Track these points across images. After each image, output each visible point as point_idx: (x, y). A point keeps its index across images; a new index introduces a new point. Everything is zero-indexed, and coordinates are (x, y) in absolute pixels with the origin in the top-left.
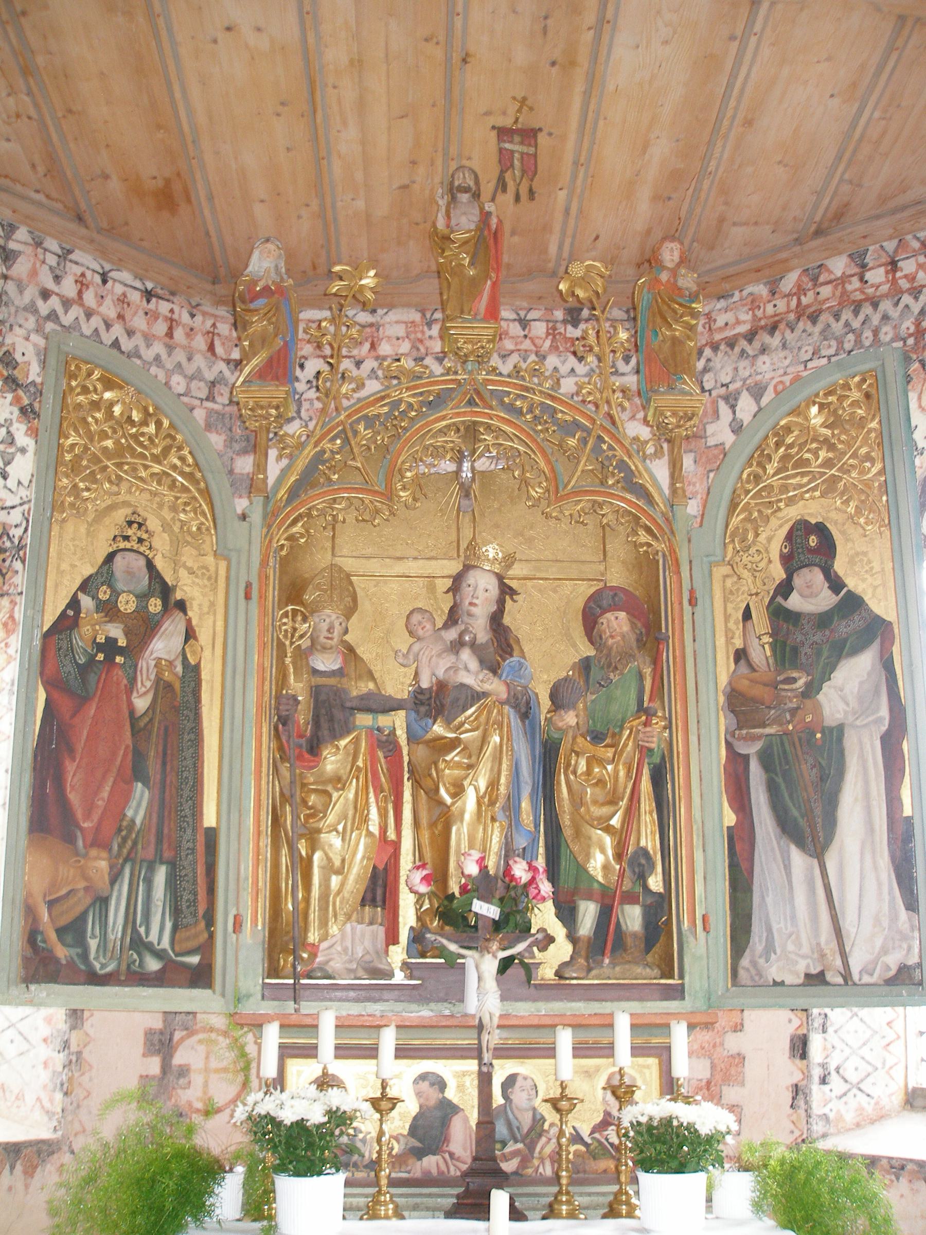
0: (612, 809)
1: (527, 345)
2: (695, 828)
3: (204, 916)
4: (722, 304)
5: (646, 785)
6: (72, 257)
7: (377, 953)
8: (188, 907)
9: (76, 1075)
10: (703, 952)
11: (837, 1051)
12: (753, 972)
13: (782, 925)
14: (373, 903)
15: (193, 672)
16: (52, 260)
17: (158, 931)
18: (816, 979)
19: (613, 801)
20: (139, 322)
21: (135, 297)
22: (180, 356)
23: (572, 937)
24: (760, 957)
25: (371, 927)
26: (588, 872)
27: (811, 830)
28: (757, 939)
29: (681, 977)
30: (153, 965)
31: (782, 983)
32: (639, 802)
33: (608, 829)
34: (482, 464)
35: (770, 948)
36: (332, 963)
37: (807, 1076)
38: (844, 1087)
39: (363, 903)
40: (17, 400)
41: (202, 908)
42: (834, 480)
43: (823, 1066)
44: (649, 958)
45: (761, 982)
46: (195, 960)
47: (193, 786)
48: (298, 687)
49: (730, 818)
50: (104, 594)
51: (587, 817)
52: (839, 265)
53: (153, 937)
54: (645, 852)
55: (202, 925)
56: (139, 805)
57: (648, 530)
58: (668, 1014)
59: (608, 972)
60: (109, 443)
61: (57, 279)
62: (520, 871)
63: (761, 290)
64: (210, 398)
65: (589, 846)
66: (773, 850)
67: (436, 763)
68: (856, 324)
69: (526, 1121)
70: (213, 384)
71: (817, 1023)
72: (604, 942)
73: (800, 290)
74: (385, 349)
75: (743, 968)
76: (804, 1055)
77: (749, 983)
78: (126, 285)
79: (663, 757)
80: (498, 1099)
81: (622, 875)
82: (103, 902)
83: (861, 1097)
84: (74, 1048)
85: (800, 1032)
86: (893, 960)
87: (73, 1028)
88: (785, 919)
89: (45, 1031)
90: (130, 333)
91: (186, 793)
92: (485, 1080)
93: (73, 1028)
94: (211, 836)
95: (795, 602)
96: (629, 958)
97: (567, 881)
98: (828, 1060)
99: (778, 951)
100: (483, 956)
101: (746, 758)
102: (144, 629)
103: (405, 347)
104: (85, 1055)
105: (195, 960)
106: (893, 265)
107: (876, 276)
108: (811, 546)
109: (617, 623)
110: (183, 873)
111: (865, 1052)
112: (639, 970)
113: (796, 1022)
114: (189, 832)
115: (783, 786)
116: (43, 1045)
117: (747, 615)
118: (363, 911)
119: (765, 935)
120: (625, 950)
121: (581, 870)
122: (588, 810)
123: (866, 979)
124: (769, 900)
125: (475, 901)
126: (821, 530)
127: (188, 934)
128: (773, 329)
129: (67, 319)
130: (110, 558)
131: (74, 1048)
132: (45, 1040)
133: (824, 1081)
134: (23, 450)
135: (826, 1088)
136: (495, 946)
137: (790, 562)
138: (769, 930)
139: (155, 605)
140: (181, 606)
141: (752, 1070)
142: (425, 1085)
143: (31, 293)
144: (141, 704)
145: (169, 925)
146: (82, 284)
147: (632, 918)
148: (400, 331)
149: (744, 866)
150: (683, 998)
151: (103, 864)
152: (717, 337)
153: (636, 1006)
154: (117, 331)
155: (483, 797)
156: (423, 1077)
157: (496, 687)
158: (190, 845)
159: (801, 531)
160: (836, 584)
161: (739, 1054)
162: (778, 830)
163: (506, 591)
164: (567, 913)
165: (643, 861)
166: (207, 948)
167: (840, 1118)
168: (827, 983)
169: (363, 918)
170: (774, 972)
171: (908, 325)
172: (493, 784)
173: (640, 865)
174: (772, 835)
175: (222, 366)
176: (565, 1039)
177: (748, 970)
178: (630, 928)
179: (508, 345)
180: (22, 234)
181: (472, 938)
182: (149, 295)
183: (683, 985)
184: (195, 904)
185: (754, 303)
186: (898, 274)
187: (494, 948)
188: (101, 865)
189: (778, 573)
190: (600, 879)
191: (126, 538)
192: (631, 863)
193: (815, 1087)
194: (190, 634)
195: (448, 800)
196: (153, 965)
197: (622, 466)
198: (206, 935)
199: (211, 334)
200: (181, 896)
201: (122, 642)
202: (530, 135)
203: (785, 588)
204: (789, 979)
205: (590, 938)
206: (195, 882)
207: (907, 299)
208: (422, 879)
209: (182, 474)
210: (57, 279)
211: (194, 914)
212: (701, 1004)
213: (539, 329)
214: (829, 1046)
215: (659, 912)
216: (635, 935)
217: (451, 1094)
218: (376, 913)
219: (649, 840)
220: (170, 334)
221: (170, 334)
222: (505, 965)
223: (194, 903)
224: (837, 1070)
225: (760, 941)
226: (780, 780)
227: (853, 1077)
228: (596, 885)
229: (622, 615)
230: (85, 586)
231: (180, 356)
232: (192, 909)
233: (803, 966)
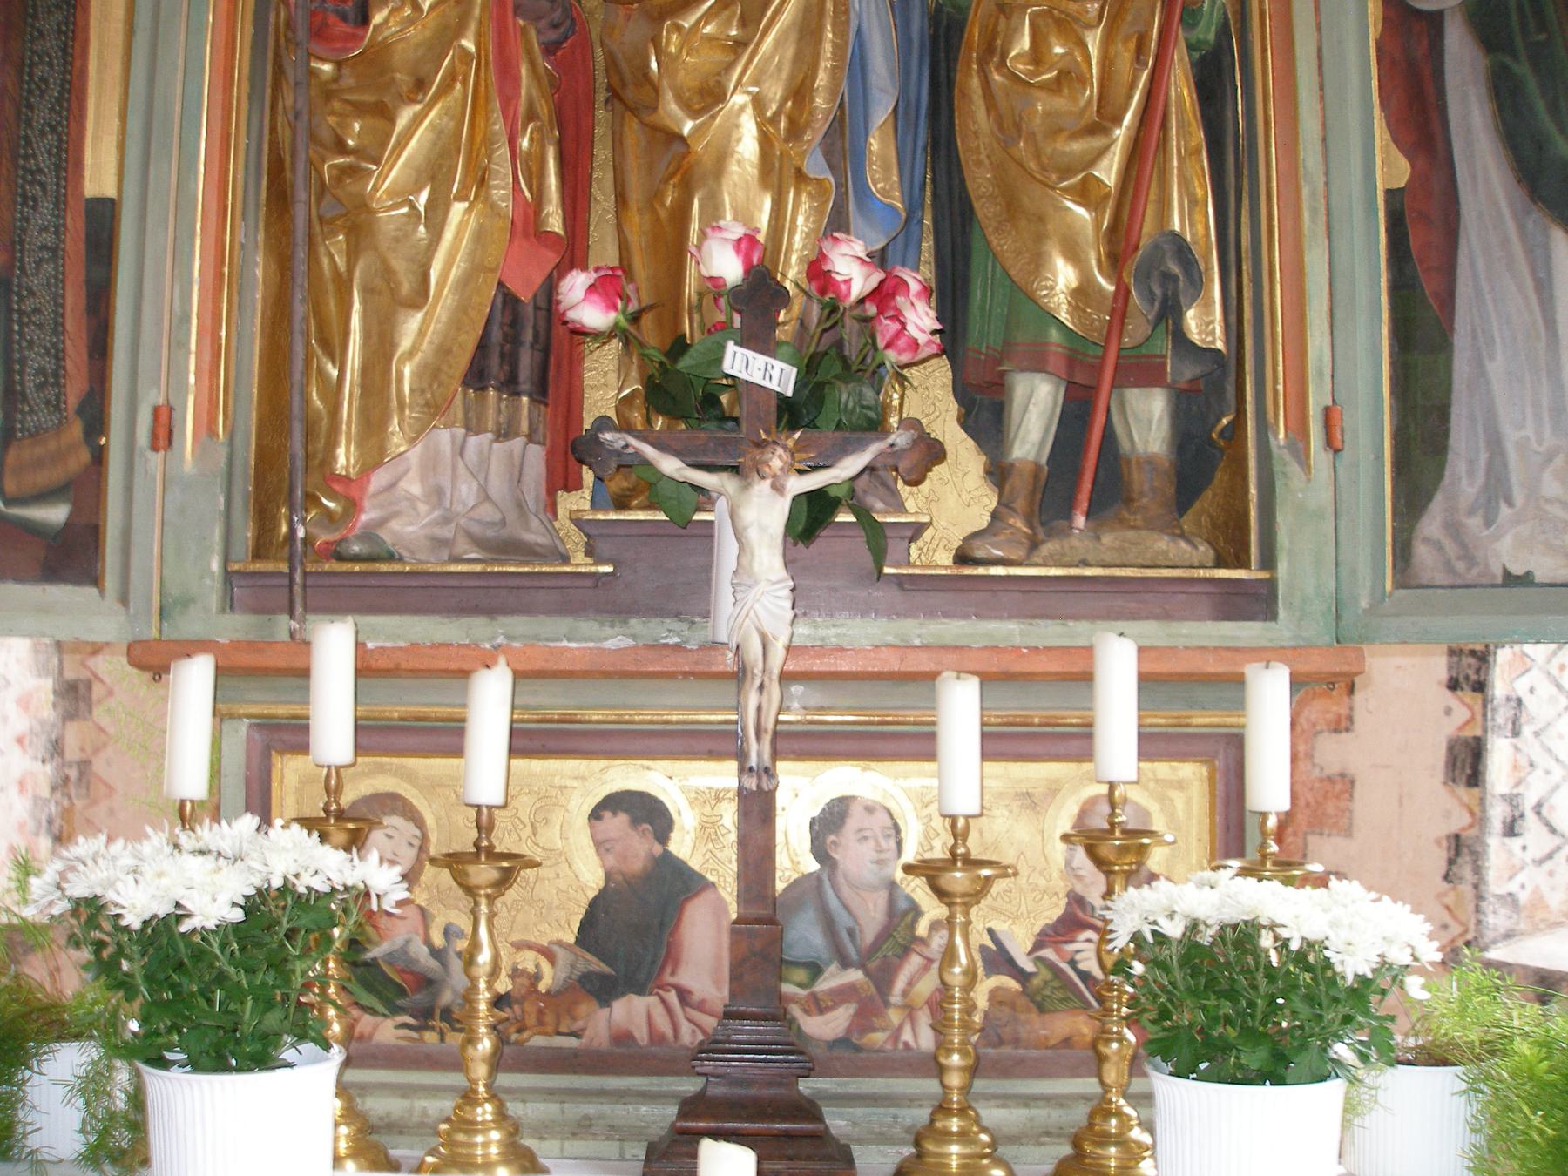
0: (1097, 142)
2: (1305, 191)
3: (80, 412)
5: (1181, 88)
7: (520, 505)
8: (40, 387)
9: (79, 804)
10: (1323, 501)
11: (1539, 772)
12: (1451, 549)
13: (1529, 431)
14: (510, 385)
19: (1102, 124)
23: (998, 473)
24: (1471, 512)
25: (507, 444)
26: (1034, 301)
28: (1462, 467)
29: (1268, 562)
31: (1526, 580)
32: (1164, 126)
33: (1087, 193)
35: (1496, 490)
36: (394, 525)
37: (1479, 818)
38: (1550, 842)
39: (476, 377)
41: (74, 391)
43: (1512, 800)
44: (1187, 522)
45: (1473, 575)
46: (56, 514)
47: (59, 100)
49: (1394, 169)
51: (1032, 165)
54: (1181, 249)
55: (76, 430)
58: (1237, 650)
59: (1085, 547)
62: (852, 270)
65: (1040, 238)
66: (1505, 243)
67: (656, 41)
69: (871, 915)
71: (1502, 716)
72: (1074, 482)
75: (1427, 540)
76: (1475, 777)
77: (1440, 578)
79: (1224, 30)
81: (1120, 307)
84: (72, 752)
85: (1468, 733)
87: (69, 716)
88: (1537, 416)
89: (20, 723)
91: (40, 115)
92: (757, 809)
93: (69, 716)
94: (103, 215)
96: (1138, 519)
97: (982, 333)
98: (1520, 790)
99: (1519, 497)
100: (746, 487)
101: (1435, 21)
104: (99, 766)
105: (56, 514)
110: (28, 306)
112: (1163, 544)
113: (1461, 714)
114: (47, 206)
115: (1532, 85)
116: (17, 750)
118: (481, 401)
119: (1483, 457)
120: (1129, 501)
121: (1023, 300)
122: (1038, 155)
124: (1496, 368)
125: (731, 347)
127: (39, 451)
131: (72, 752)
132: (20, 741)
133: (1511, 830)
135: (1515, 844)
136: (777, 461)
138: (1495, 443)
141: (1369, 805)
142: (616, 824)
147: (1147, 421)
149: (1429, 286)
150: (1271, 615)
153: (1155, 632)
155: (774, 120)
156: (614, 803)
158: (48, 239)
161: (1342, 775)
162: (1520, 194)
164: (985, 413)
165: (1175, 268)
166: (86, 488)
167: (1538, 902)
169: (481, 417)
172: (800, 92)
173: (1167, 277)
174: (1506, 211)
176: (960, 707)
177: (1439, 547)
178: (1140, 447)
181: (724, 443)
183: (1271, 584)
187: (776, 464)
190: (1064, 316)
192: (1143, 276)
193: (1495, 843)
195: (687, 127)
198: (85, 456)
200: (23, 361)
205: (1037, 467)
206: (58, 327)
208: (592, 289)
211: (57, 405)
212: (1318, 630)
214: (1524, 762)
216: (1150, 461)
217: (681, 845)
218: (518, 409)
219: (1187, 213)
222: (812, 515)
223: (55, 378)
224: (1538, 809)
225: (1471, 473)
226: (1523, 69)
228: (1054, 335)
232: (51, 392)
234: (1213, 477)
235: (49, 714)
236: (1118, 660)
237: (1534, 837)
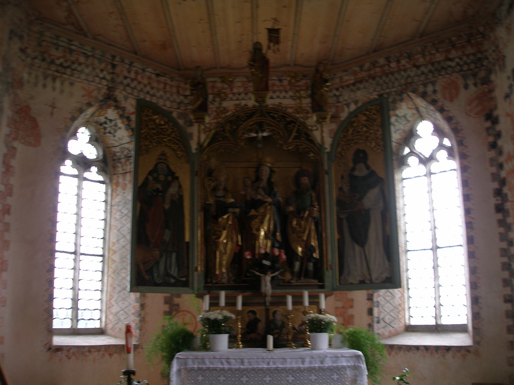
1: (281, 88)
4: (345, 73)
5: (313, 227)
6: (133, 65)
10: (330, 275)
15: (181, 198)
16: (127, 66)
17: (174, 271)
18: (362, 282)
20: (155, 85)
21: (153, 76)
22: (168, 95)
27: (360, 239)
30: (172, 281)
34: (265, 134)
37: (373, 321)
38: (385, 324)
40: (118, 113)
42: (368, 137)
43: (378, 318)
46: (184, 279)
48: (211, 201)
50: (155, 175)
52: (382, 61)
53: (172, 273)
56: (167, 235)
57: (314, 153)
59: (303, 281)
60: (154, 131)
61: (129, 72)
62: (276, 252)
63: (357, 69)
64: (178, 108)
68: (387, 81)
69: (279, 323)
70: (179, 103)
71: (376, 304)
73: (370, 69)
74: (235, 90)
78: (151, 73)
80: (271, 318)
82: (157, 263)
83: (391, 328)
86: (385, 275)
89: (133, 311)
90: (152, 88)
92: (267, 310)
95: (356, 173)
102: (167, 185)
103: (241, 90)
105: (184, 279)
106: (398, 62)
107: (393, 65)
108: (361, 157)
109: (305, 180)
111: (392, 314)
117: (342, 177)
123: (377, 282)
126: (364, 152)
128: (361, 82)
129: (133, 85)
130: (156, 165)
134: (120, 128)
135: (379, 324)
136: (269, 273)
137: (356, 161)
139: (170, 178)
140: (177, 178)
143: (121, 79)
144: (167, 207)
145: (177, 269)
146: (137, 73)
148: (239, 84)
151: (158, 252)
152: (344, 84)
153: (311, 290)
154: (148, 88)
157: (269, 200)
159: (359, 152)
160: (368, 167)
163: (272, 171)
166: (187, 276)
167: (383, 334)
168: (365, 283)
170: (351, 280)
171: (403, 81)
172: (269, 228)
175: (182, 98)
176: (290, 299)
179: (275, 88)
180: (117, 59)
182: (158, 75)
185: (355, 73)
186: (401, 64)
188: (157, 253)
189: (351, 165)
191: (161, 159)
193: (376, 325)
194: (180, 187)
196: (172, 281)
197: (306, 134)
199: (178, 87)
201: (161, 189)
202: (277, 31)
203: (353, 169)
204: (355, 282)
207: (403, 73)
209: (177, 140)
210: (129, 72)
213: (285, 83)
215: (319, 264)
217: (258, 316)
219: (314, 243)
220: (165, 88)
221: (165, 88)
222: (273, 278)
227: (387, 321)
229: (306, 178)
230: (150, 173)
231: (168, 95)
233: (359, 278)
235: (138, 309)
236: (306, 294)
237: (382, 324)
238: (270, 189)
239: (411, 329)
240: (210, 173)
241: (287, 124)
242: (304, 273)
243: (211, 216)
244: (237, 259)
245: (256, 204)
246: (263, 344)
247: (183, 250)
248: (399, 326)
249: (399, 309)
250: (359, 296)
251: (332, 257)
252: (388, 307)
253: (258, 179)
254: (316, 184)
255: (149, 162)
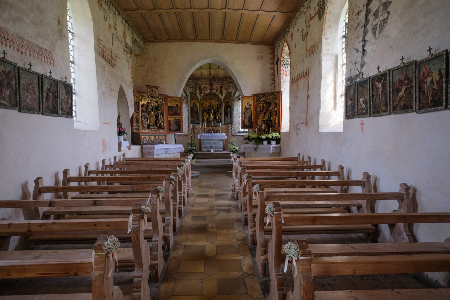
27: (227, 116)
102: (195, 107)
108: (228, 102)
184: (199, 120)
234: (221, 122)
238: (213, 108)
239: (239, 132)
240: (202, 104)
241: (215, 96)
242: (218, 122)
243: (203, 112)
244: (207, 119)
245: (210, 110)
246: (212, 133)
247: (198, 118)
248: (238, 131)
249: (237, 128)
250: (230, 125)
251: (223, 119)
252: (235, 128)
253: (211, 105)
254: (221, 106)
255: (192, 103)
